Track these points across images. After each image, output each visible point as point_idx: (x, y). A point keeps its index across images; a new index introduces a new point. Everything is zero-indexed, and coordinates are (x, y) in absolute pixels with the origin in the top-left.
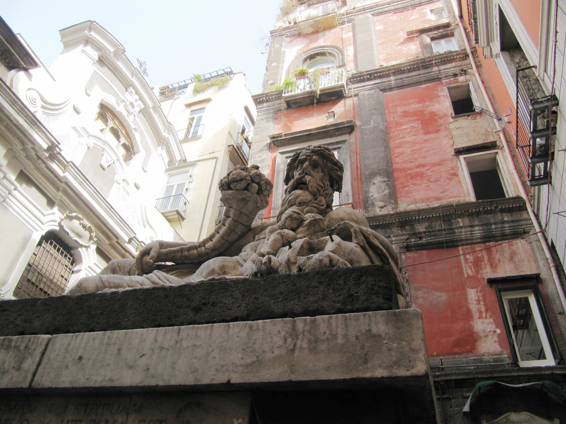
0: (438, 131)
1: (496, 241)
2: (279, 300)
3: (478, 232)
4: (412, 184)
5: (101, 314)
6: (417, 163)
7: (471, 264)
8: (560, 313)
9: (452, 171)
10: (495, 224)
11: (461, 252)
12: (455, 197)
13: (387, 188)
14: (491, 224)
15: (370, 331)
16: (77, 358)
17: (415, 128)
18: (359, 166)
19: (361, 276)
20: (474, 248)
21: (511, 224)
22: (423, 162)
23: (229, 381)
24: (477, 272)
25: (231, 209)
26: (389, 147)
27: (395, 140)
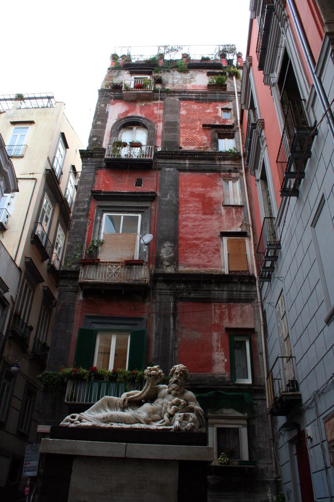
0: (212, 214)
1: (235, 302)
3: (225, 295)
4: (190, 251)
6: (195, 236)
7: (217, 316)
8: (260, 353)
9: (216, 247)
10: (236, 291)
11: (213, 309)
12: (216, 267)
13: (173, 252)
14: (233, 291)
17: (198, 207)
18: (155, 230)
20: (220, 306)
21: (245, 293)
22: (199, 236)
24: (220, 321)
26: (178, 219)
27: (183, 214)
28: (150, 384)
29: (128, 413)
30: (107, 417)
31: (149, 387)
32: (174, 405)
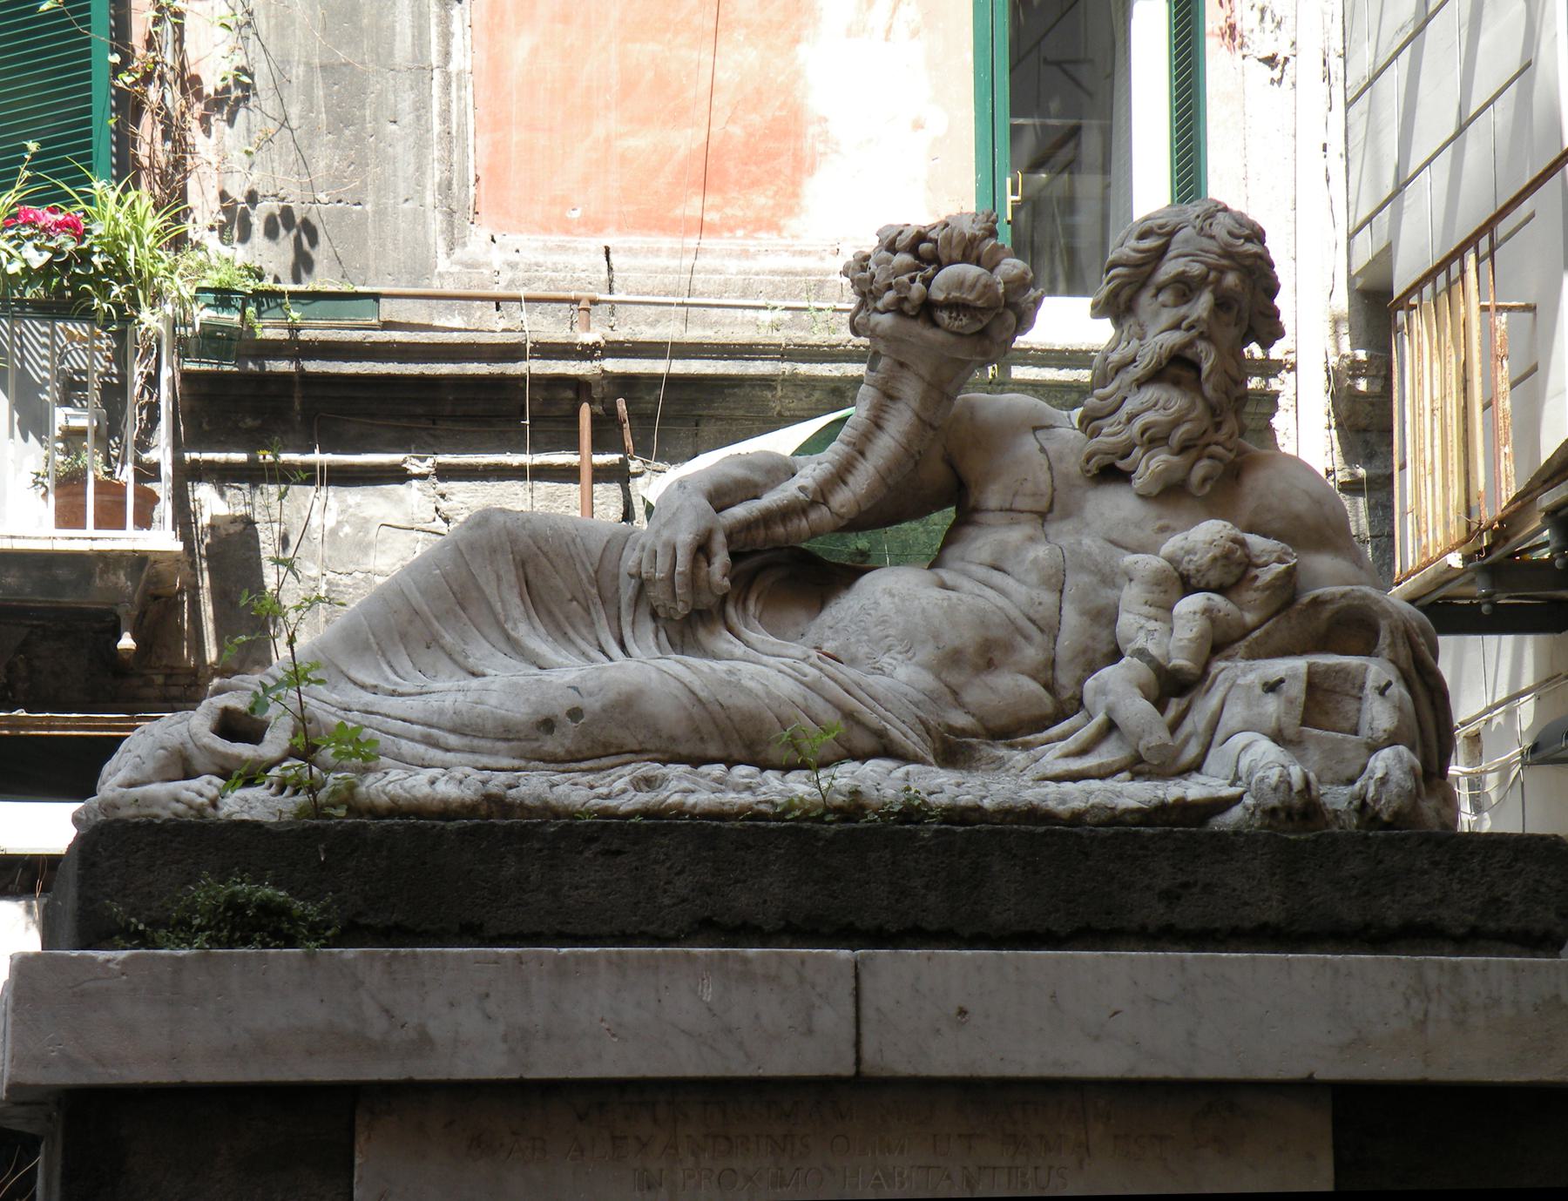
2: (1354, 893)
5: (926, 887)
15: (1557, 997)
16: (954, 1011)
19: (1516, 860)
23: (1311, 1076)
25: (906, 373)
28: (911, 391)
29: (760, 664)
30: (575, 714)
31: (899, 423)
32: (1187, 585)
